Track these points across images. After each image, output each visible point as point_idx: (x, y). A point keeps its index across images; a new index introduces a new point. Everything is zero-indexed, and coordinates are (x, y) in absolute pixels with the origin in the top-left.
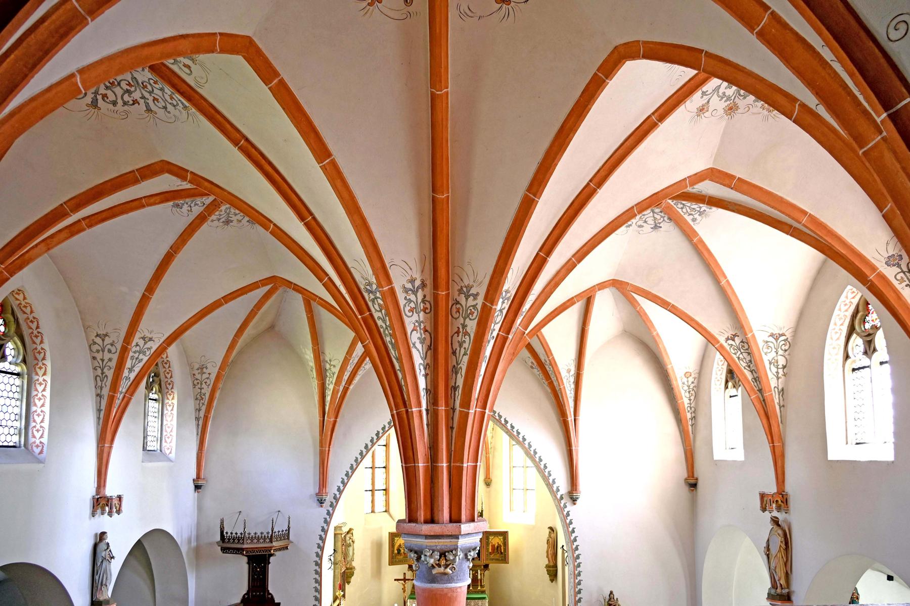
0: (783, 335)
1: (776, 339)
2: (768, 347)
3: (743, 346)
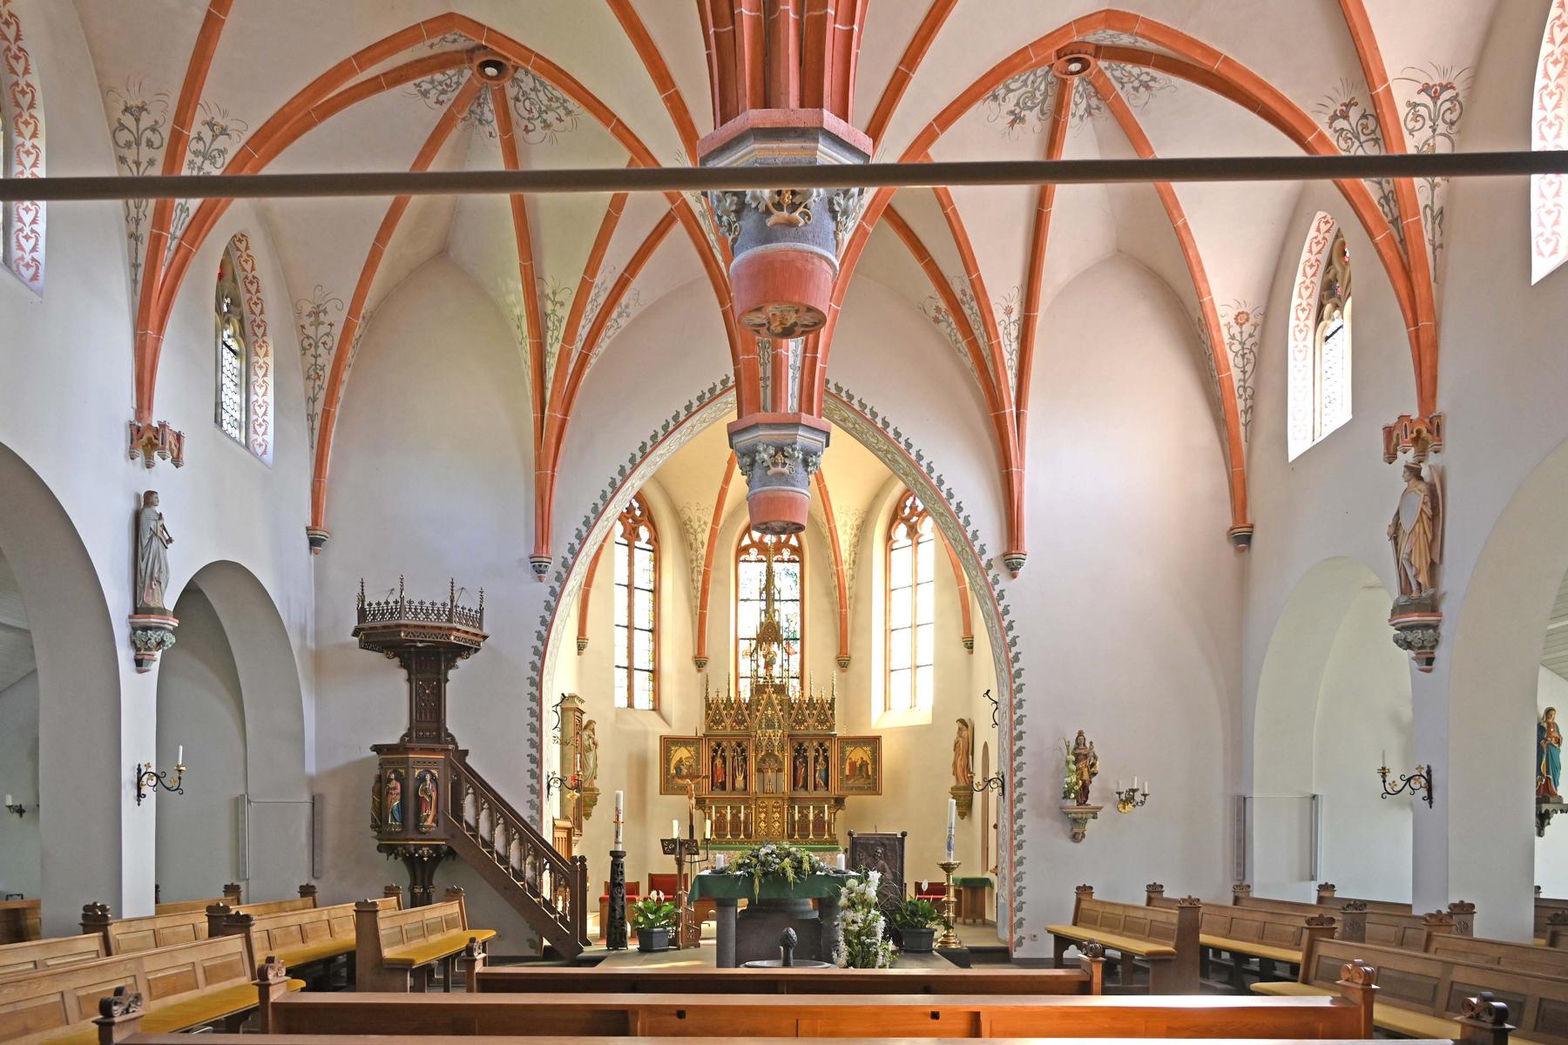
0: (1448, 86)
1: (1435, 98)
2: (1417, 117)
3: (1365, 127)
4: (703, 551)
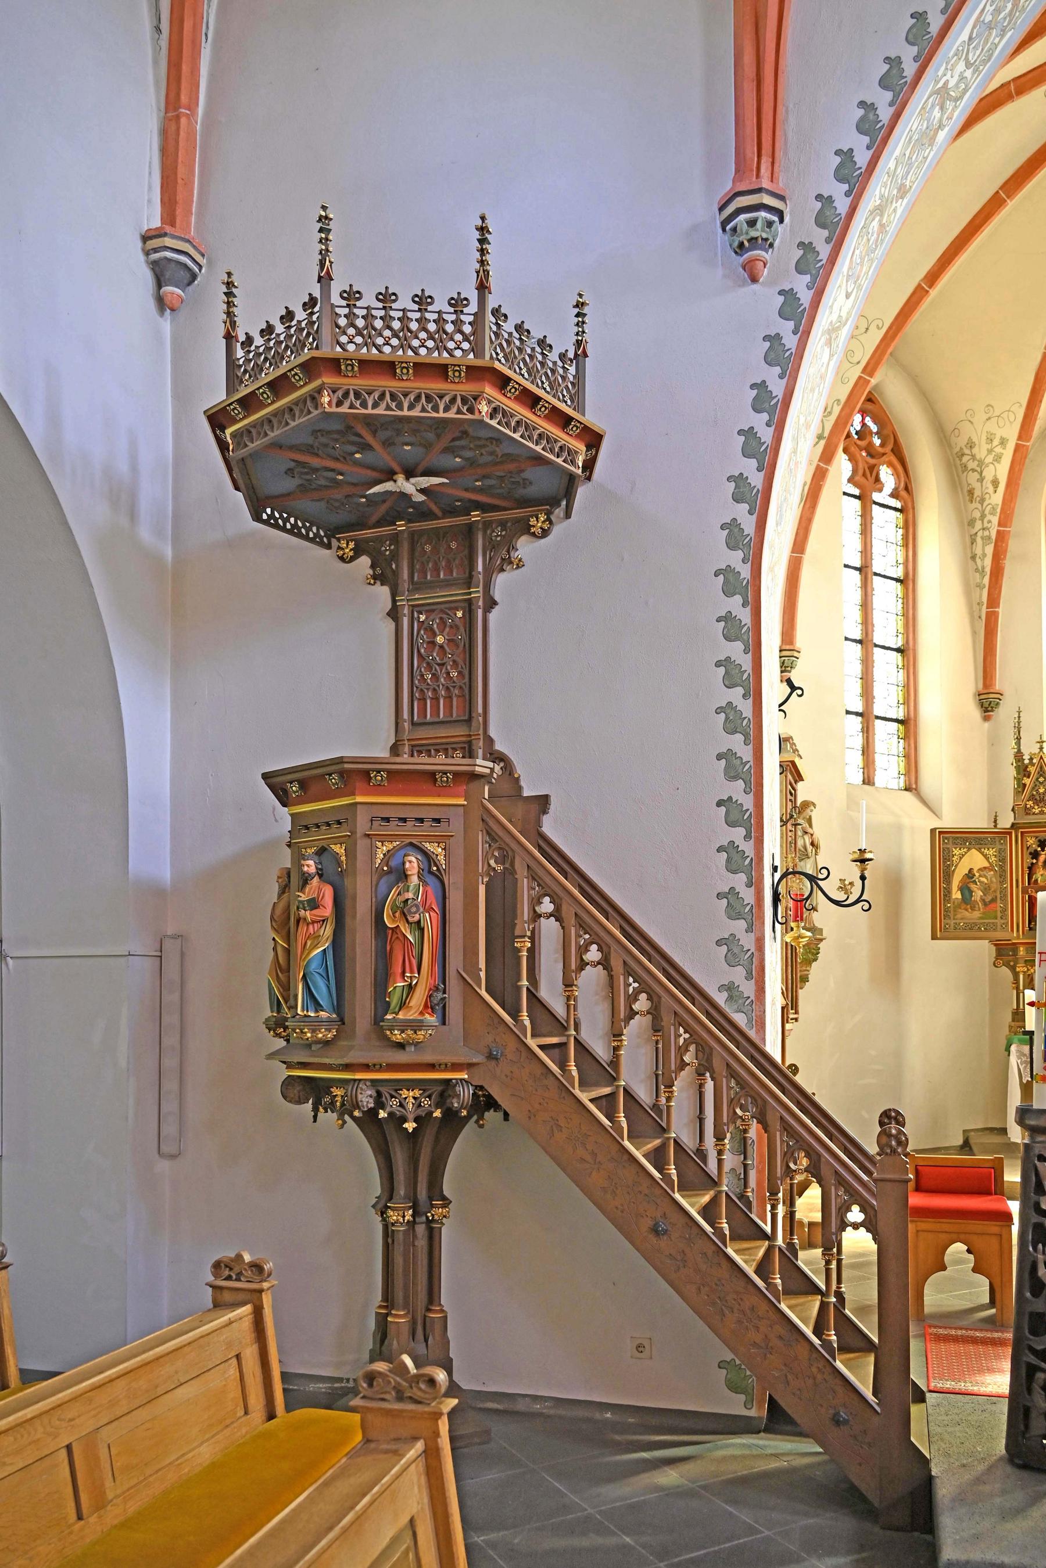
4: (997, 499)
